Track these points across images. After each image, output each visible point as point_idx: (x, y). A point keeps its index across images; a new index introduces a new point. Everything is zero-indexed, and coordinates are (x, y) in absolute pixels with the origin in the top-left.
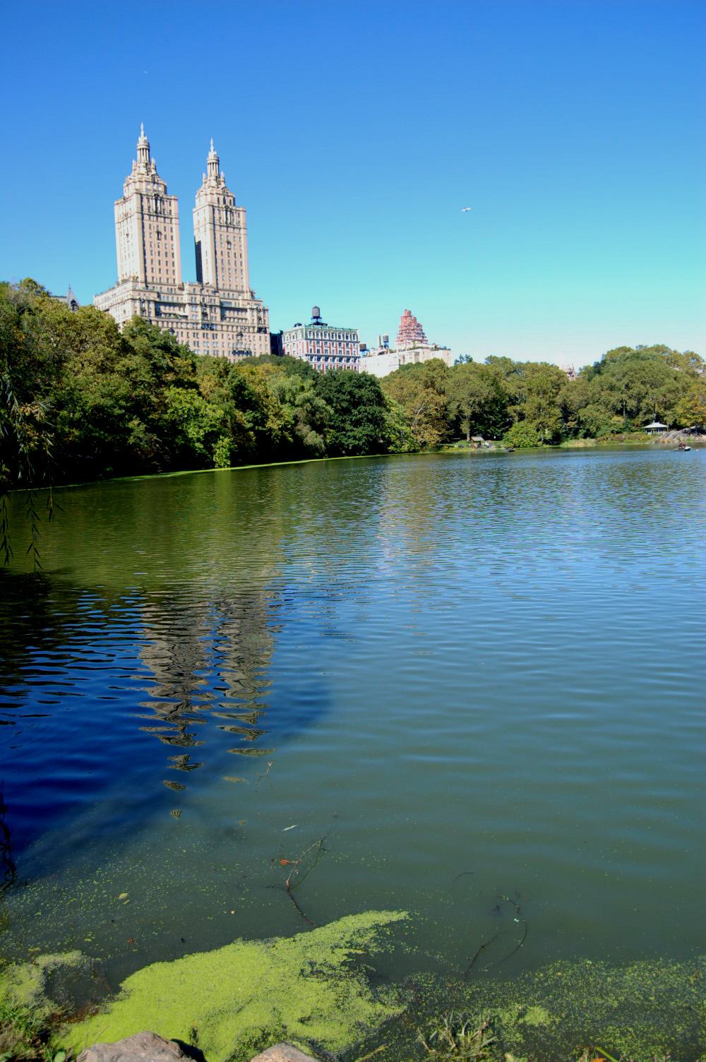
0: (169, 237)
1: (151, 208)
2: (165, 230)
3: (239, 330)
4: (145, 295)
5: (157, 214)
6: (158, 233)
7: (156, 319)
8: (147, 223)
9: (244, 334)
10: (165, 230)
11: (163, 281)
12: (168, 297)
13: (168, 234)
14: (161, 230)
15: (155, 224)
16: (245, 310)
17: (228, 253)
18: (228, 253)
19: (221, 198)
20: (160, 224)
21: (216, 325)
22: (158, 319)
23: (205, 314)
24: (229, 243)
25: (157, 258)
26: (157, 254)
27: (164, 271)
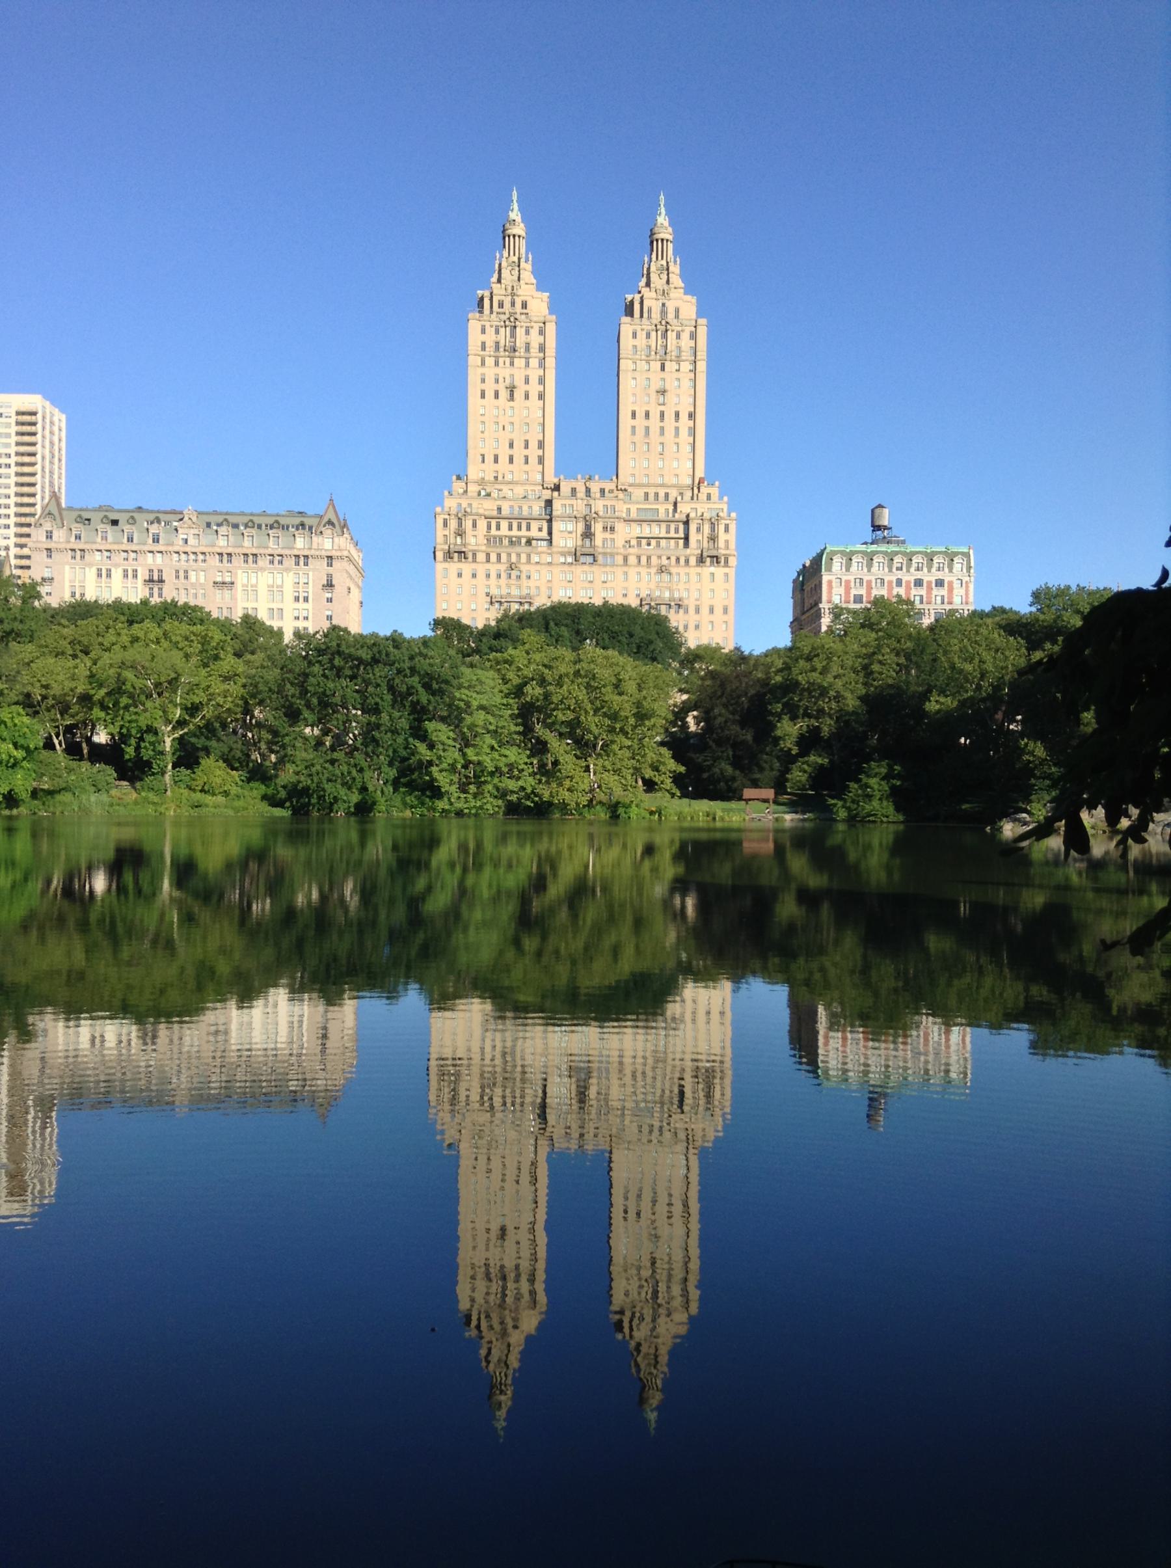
0: (534, 395)
1: (502, 344)
2: (527, 381)
3: (665, 562)
4: (470, 505)
6: (512, 390)
7: (484, 548)
9: (674, 570)
10: (527, 381)
12: (520, 508)
14: (519, 381)
17: (662, 414)
18: (662, 414)
21: (612, 555)
22: (489, 550)
23: (588, 534)
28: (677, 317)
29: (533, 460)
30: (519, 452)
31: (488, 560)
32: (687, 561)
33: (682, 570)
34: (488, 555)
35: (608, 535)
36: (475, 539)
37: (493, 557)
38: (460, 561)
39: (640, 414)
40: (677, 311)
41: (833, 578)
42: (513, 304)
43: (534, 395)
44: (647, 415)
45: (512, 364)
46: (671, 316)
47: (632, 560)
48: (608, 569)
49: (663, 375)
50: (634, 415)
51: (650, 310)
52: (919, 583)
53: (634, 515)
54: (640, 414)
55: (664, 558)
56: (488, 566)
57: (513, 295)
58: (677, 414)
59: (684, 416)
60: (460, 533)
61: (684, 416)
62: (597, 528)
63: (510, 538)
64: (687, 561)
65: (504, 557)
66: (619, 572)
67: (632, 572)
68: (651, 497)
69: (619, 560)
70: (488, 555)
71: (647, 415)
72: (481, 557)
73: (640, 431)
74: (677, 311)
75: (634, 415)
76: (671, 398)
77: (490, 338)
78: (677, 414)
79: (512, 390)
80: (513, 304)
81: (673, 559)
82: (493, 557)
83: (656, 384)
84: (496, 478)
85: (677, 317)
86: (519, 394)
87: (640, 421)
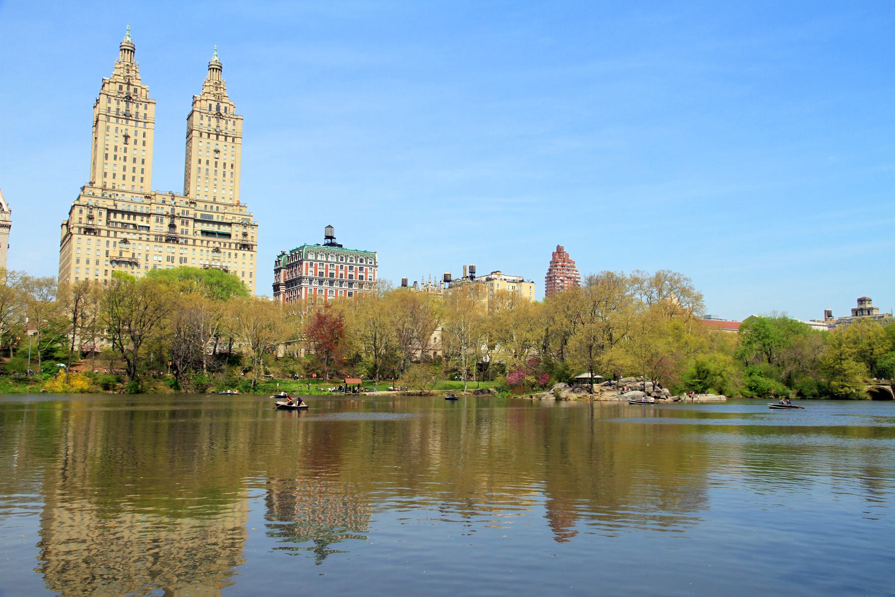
0: (140, 143)
2: (136, 134)
3: (217, 245)
5: (127, 116)
6: (127, 137)
8: (113, 127)
10: (136, 134)
13: (140, 139)
14: (131, 133)
15: (124, 128)
16: (230, 224)
17: (216, 163)
18: (216, 163)
19: (214, 105)
20: (130, 128)
23: (172, 226)
24: (217, 151)
25: (121, 163)
26: (122, 159)
28: (226, 112)
29: (138, 179)
30: (129, 174)
31: (108, 236)
32: (230, 246)
33: (228, 251)
34: (109, 232)
35: (184, 227)
36: (100, 222)
37: (112, 234)
39: (204, 162)
42: (128, 89)
43: (140, 143)
44: (208, 162)
45: (127, 123)
46: (222, 111)
47: (198, 243)
48: (184, 246)
49: (217, 142)
50: (200, 161)
53: (199, 217)
54: (204, 162)
56: (108, 239)
57: (129, 84)
58: (225, 164)
59: (228, 166)
60: (91, 218)
61: (228, 166)
62: (177, 222)
63: (123, 223)
64: (230, 246)
65: (119, 234)
66: (190, 248)
67: (198, 249)
68: (208, 209)
69: (190, 242)
70: (109, 232)
71: (208, 162)
72: (104, 233)
73: (203, 171)
74: (226, 108)
75: (200, 161)
76: (221, 155)
77: (113, 105)
78: (225, 164)
79: (127, 137)
80: (128, 89)
82: (112, 234)
83: (213, 147)
84: (114, 187)
86: (131, 141)
87: (203, 165)
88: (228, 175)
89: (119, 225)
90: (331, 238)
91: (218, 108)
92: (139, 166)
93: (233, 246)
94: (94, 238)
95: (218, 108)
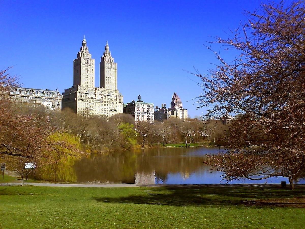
3: (113, 103)
11: (89, 86)
20: (88, 68)
27: (89, 83)
28: (112, 62)
31: (86, 101)
37: (87, 101)
38: (81, 101)
40: (112, 61)
41: (136, 107)
51: (108, 60)
52: (147, 108)
55: (113, 102)
61: (114, 78)
70: (86, 100)
72: (85, 100)
73: (108, 80)
81: (114, 103)
82: (87, 101)
85: (112, 62)
88: (114, 81)
89: (88, 98)
90: (140, 99)
91: (110, 61)
92: (91, 79)
93: (117, 103)
94: (82, 102)
95: (110, 61)
